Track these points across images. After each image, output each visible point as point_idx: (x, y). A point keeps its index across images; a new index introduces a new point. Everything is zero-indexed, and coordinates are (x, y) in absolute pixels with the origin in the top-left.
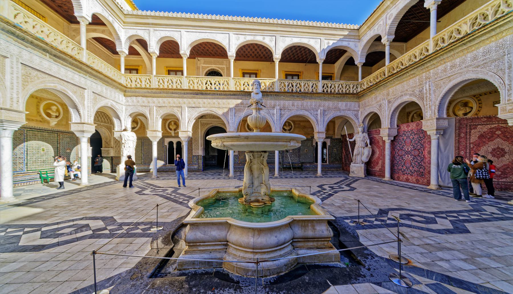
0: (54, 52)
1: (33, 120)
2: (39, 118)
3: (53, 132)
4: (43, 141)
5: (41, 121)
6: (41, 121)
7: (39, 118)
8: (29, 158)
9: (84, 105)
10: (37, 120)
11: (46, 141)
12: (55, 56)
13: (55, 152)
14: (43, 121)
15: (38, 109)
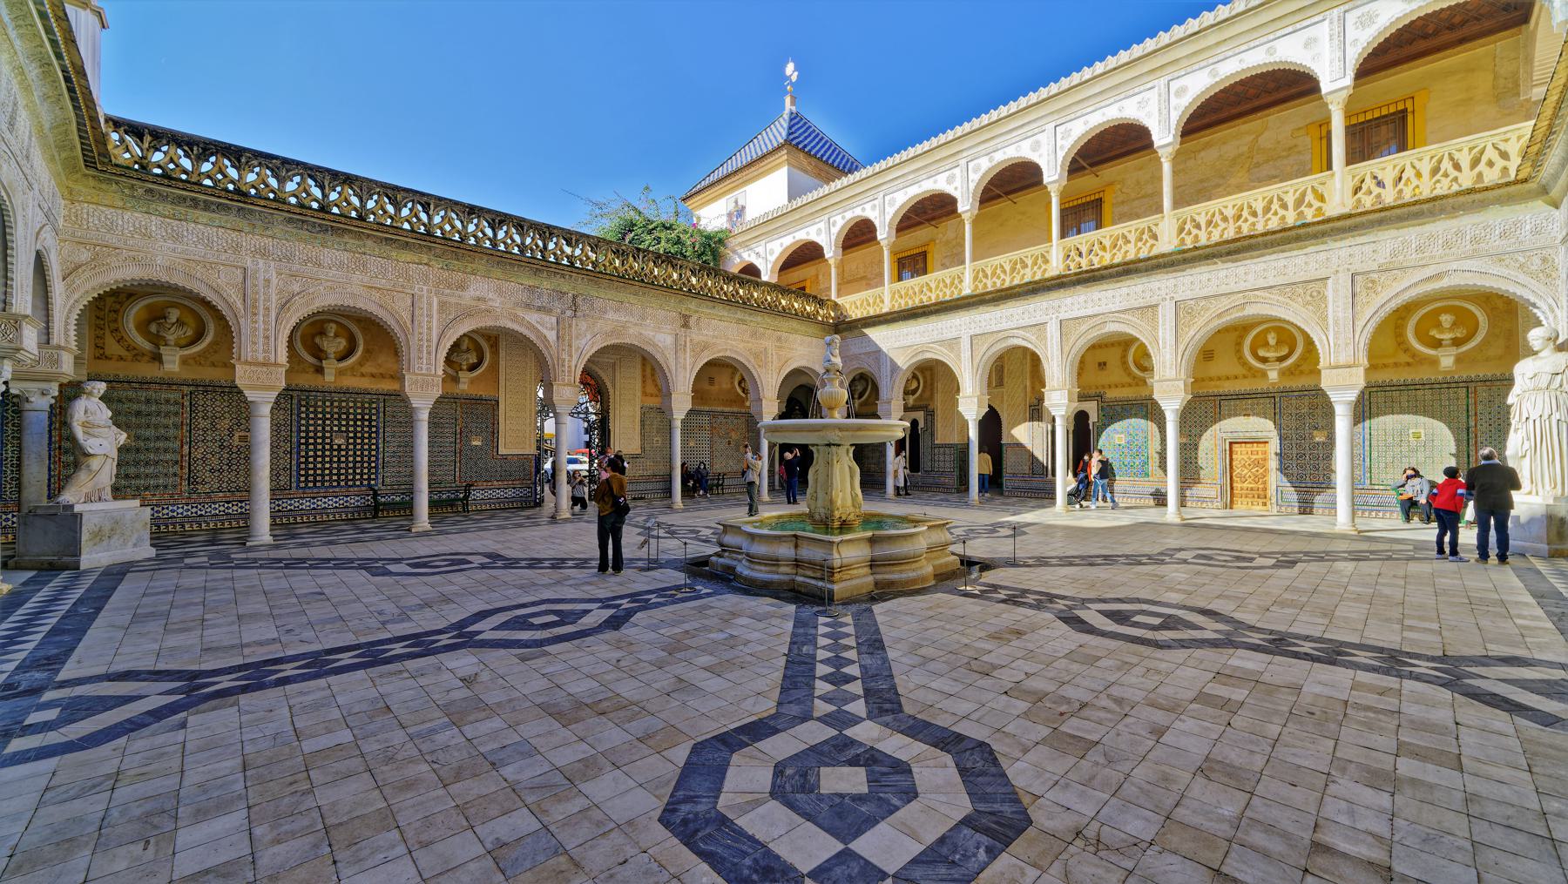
0: (1224, 248)
1: (1385, 366)
2: (1404, 358)
3: (1449, 384)
4: (1416, 413)
5: (1408, 364)
6: (1408, 364)
7: (1404, 358)
8: (1375, 454)
9: (1324, 318)
10: (1396, 365)
11: (1425, 413)
12: (1229, 254)
13: (1457, 441)
14: (1418, 360)
15: (1241, 358)
